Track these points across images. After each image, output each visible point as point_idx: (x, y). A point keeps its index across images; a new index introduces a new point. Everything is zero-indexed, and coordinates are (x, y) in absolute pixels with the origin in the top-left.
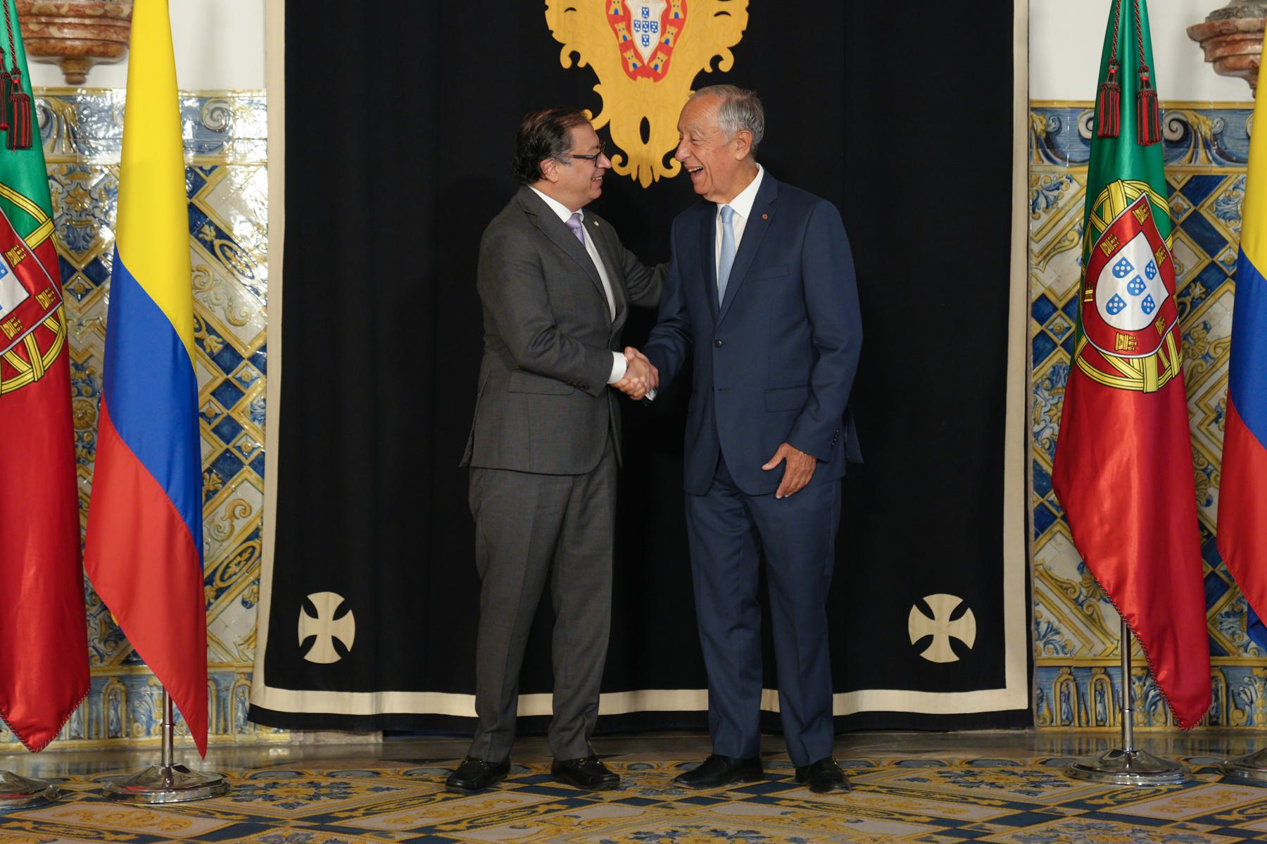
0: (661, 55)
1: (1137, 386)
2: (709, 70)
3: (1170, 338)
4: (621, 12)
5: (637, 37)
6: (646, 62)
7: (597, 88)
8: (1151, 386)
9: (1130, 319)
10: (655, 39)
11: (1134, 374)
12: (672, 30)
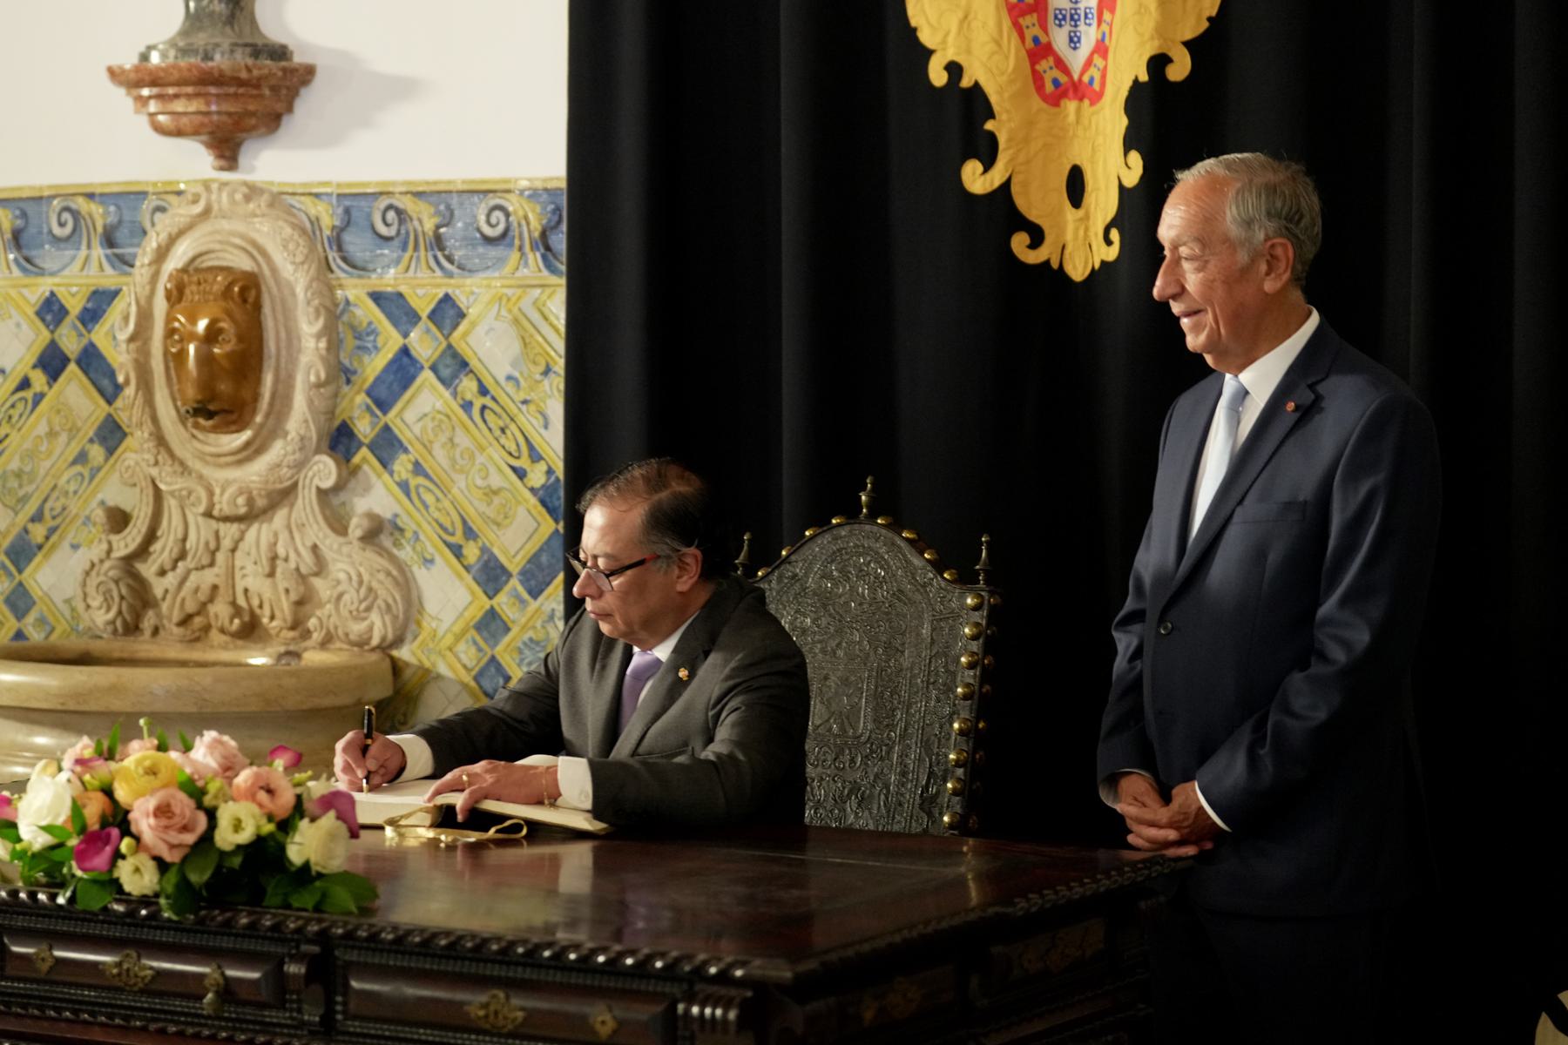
0: (1098, 60)
5: (1059, 38)
6: (1076, 77)
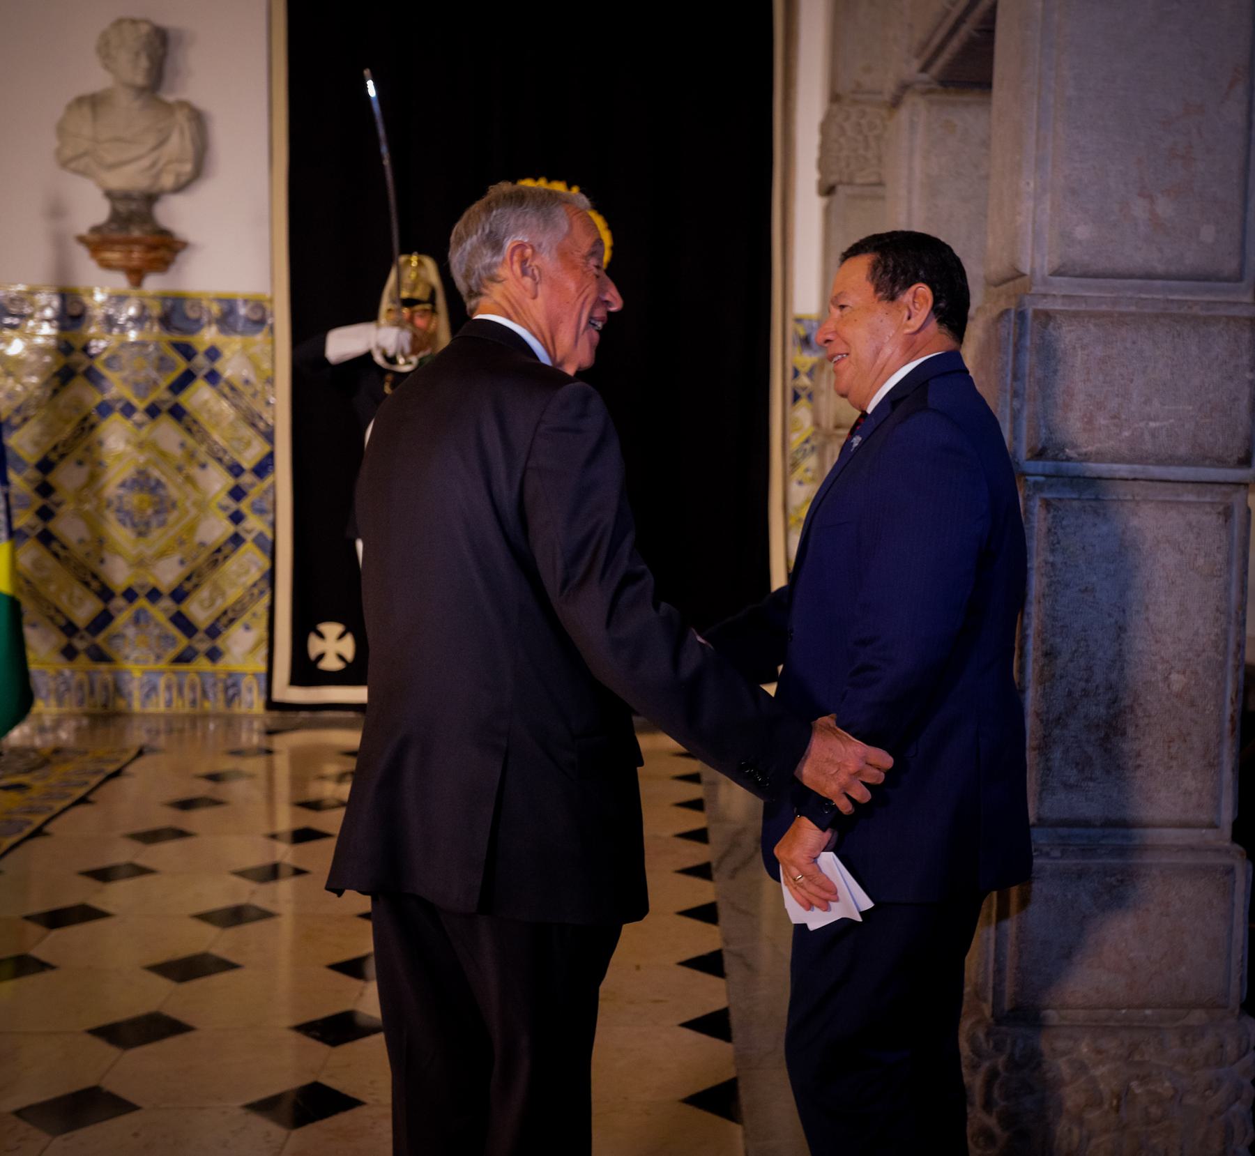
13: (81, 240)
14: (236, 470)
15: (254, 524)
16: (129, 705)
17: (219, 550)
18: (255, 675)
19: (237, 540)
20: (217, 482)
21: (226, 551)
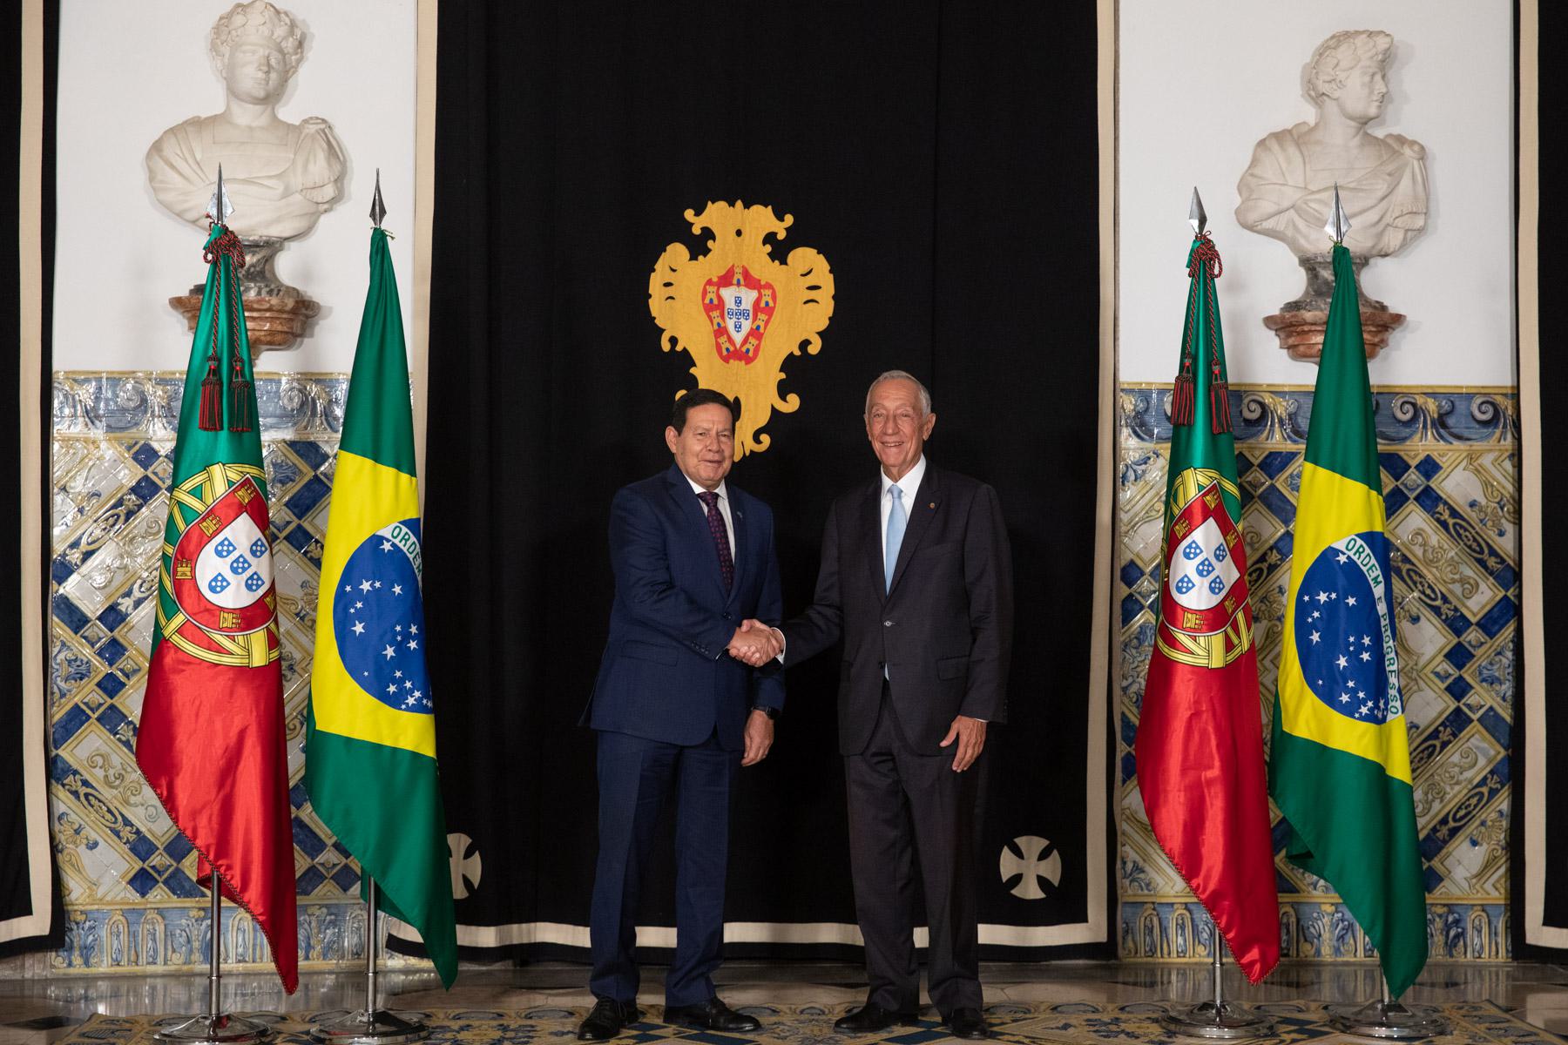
0: (753, 341)
1: (1202, 662)
2: (797, 353)
3: (1240, 616)
4: (716, 302)
5: (730, 324)
7: (692, 370)
8: (1217, 662)
9: (1197, 598)
10: (747, 325)
11: (1202, 651)
12: (762, 317)
13: (1269, 321)
14: (1457, 624)
15: (1482, 697)
16: (1318, 953)
17: (1435, 735)
18: (1484, 908)
19: (1457, 721)
20: (1430, 639)
21: (1444, 737)
